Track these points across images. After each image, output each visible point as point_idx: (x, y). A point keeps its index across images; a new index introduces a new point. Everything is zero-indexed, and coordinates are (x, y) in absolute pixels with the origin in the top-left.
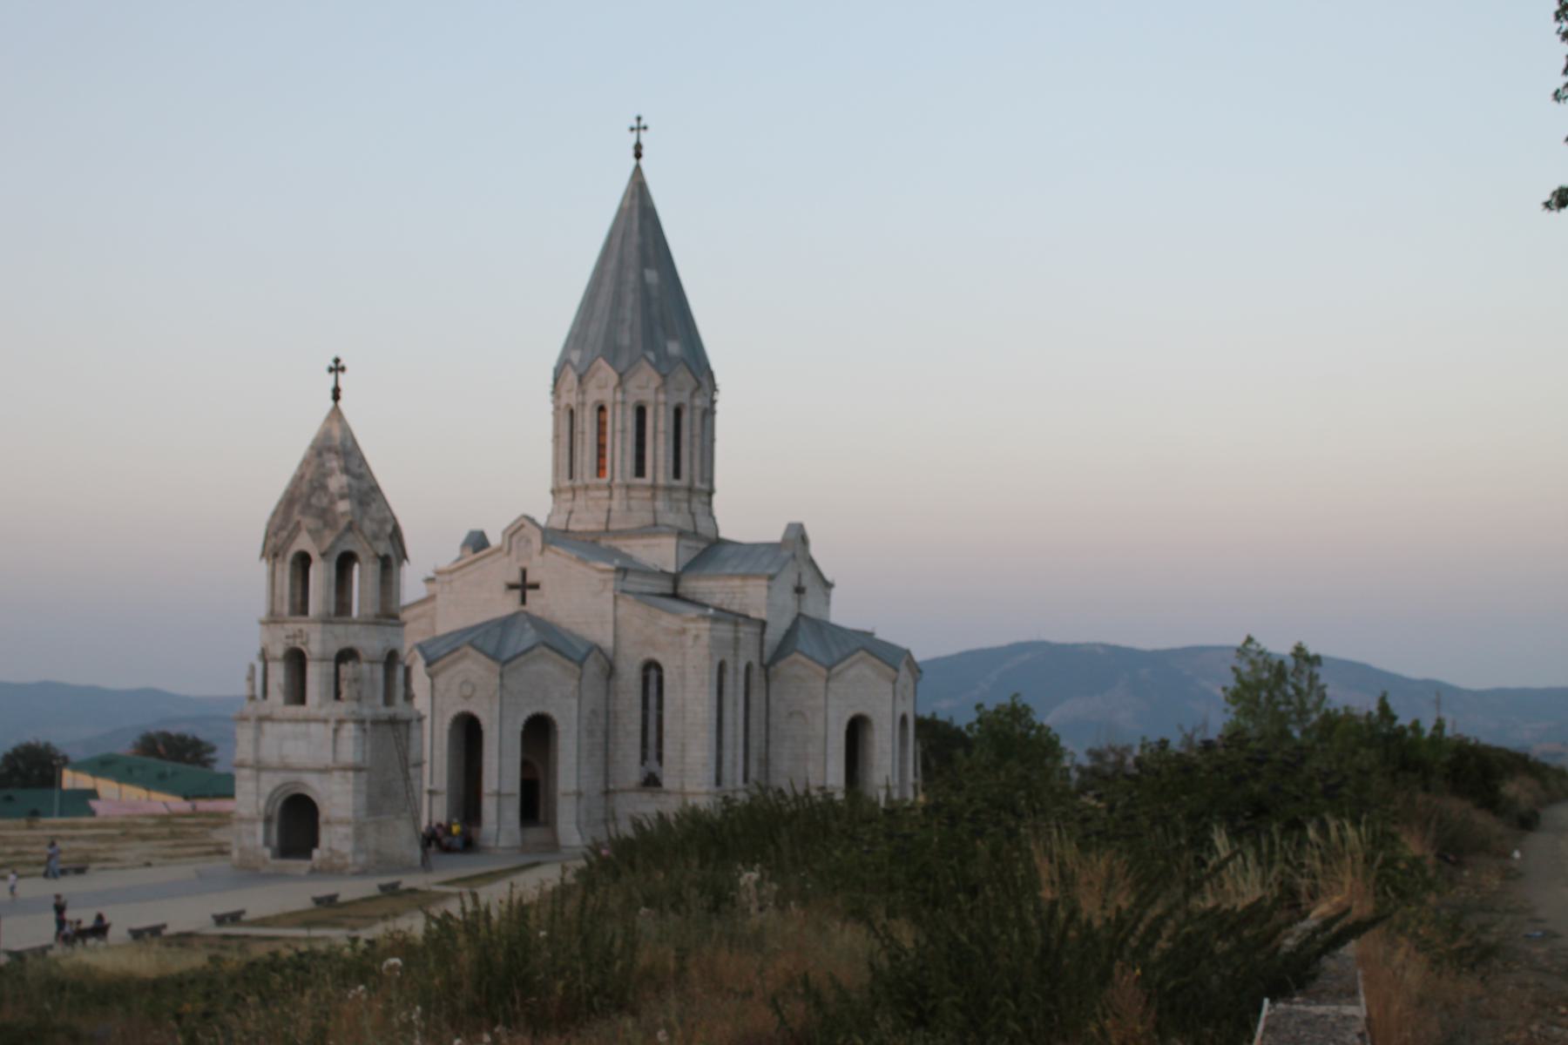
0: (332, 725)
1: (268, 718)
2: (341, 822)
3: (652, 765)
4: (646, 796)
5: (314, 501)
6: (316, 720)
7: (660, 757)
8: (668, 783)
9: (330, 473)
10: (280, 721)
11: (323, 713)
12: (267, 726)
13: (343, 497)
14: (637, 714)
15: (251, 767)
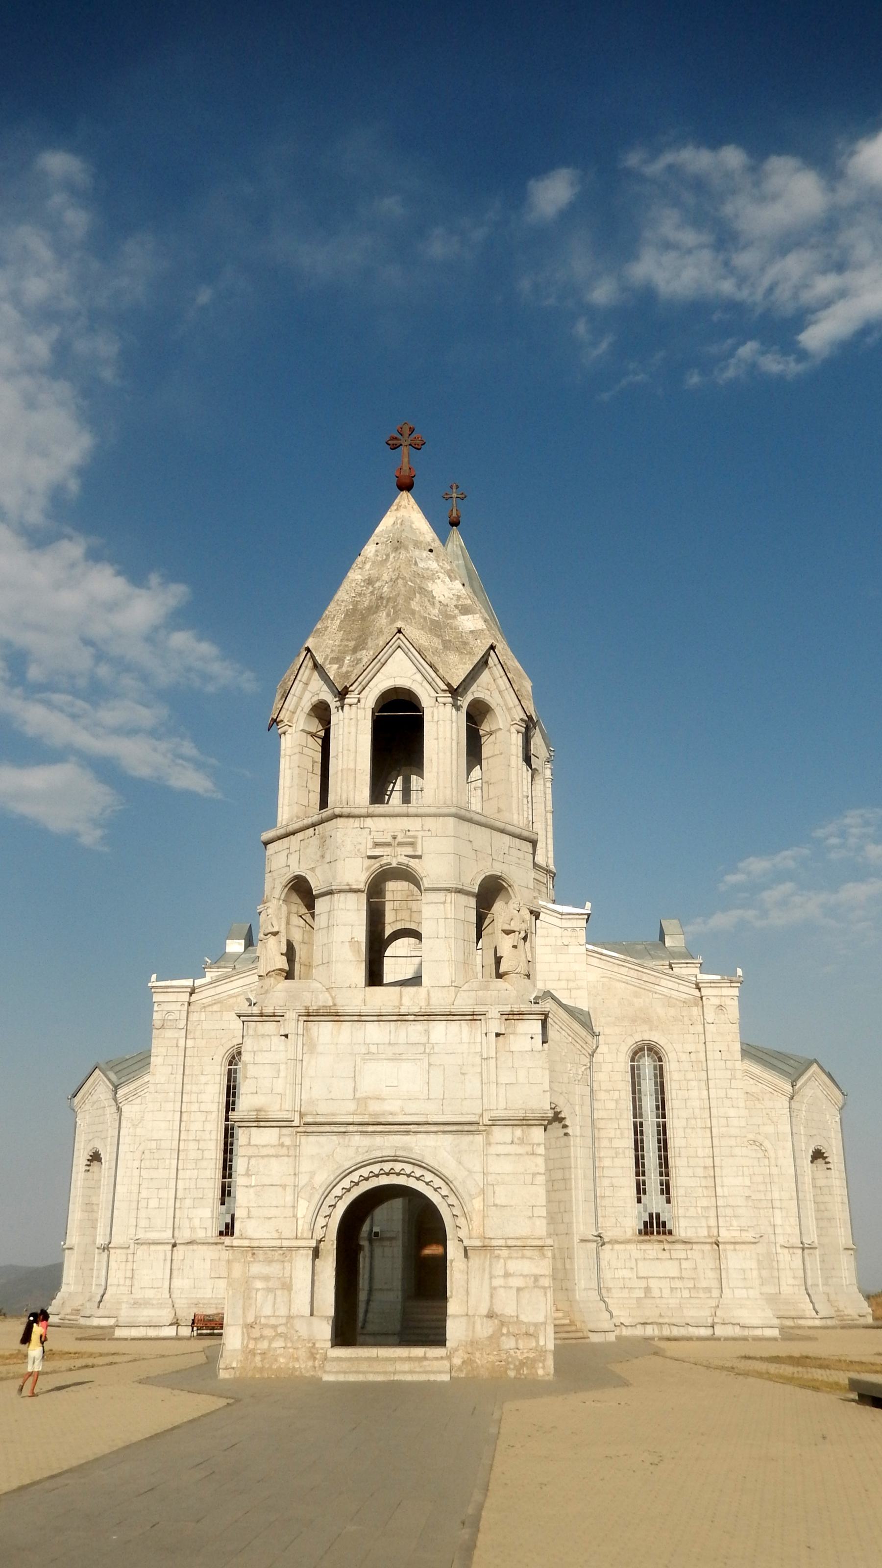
0: (495, 1026)
1: (335, 1016)
2: (519, 1247)
3: (655, 1202)
4: (652, 1248)
5: (414, 605)
6: (450, 1016)
7: (666, 1189)
8: (682, 1228)
9: (433, 577)
10: (360, 1018)
11: (464, 1003)
12: (324, 1031)
13: (465, 610)
14: (627, 1123)
15: (283, 1124)
